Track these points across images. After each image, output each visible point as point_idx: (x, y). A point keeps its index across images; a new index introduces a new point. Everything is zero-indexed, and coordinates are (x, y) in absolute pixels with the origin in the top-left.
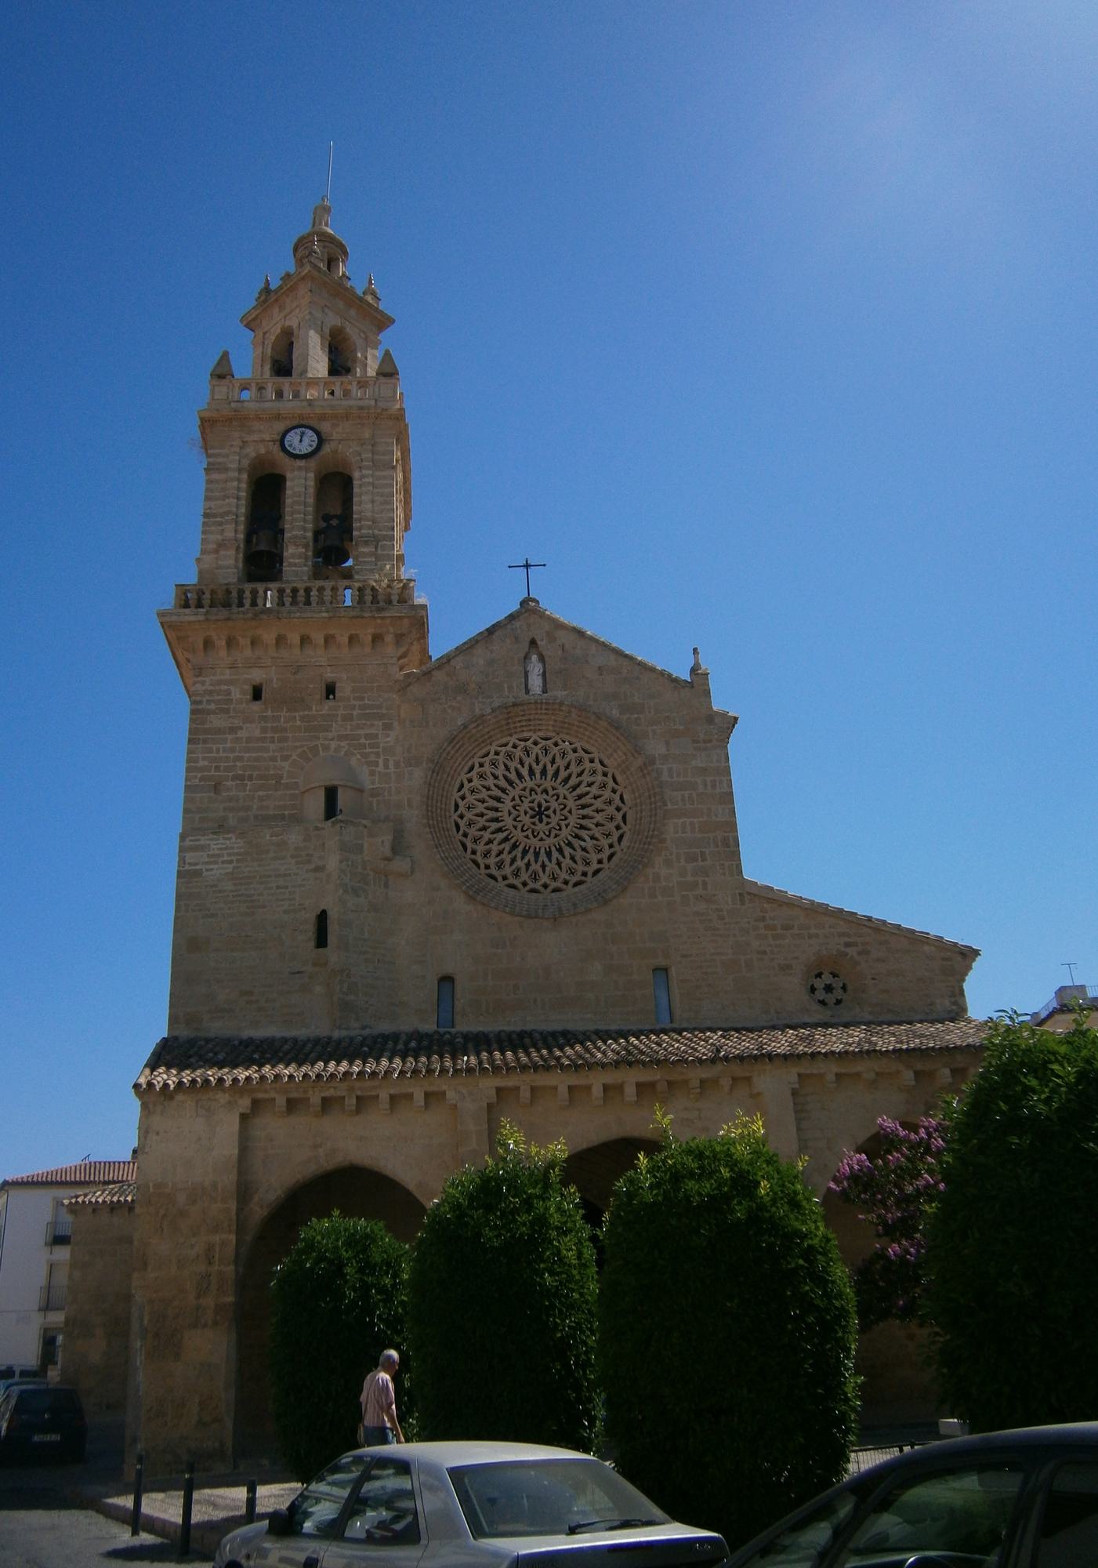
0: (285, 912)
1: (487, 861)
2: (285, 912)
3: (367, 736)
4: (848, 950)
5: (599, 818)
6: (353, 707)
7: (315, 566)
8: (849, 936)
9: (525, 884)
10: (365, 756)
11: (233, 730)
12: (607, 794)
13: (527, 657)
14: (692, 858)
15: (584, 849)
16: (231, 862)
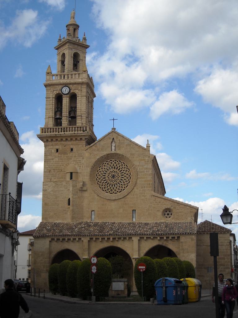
2: (62, 198)
3: (79, 161)
6: (76, 154)
7: (70, 121)
8: (172, 204)
9: (109, 192)
10: (78, 165)
11: (53, 159)
12: (127, 172)
13: (112, 142)
14: (142, 188)
15: (122, 185)
16: (52, 188)
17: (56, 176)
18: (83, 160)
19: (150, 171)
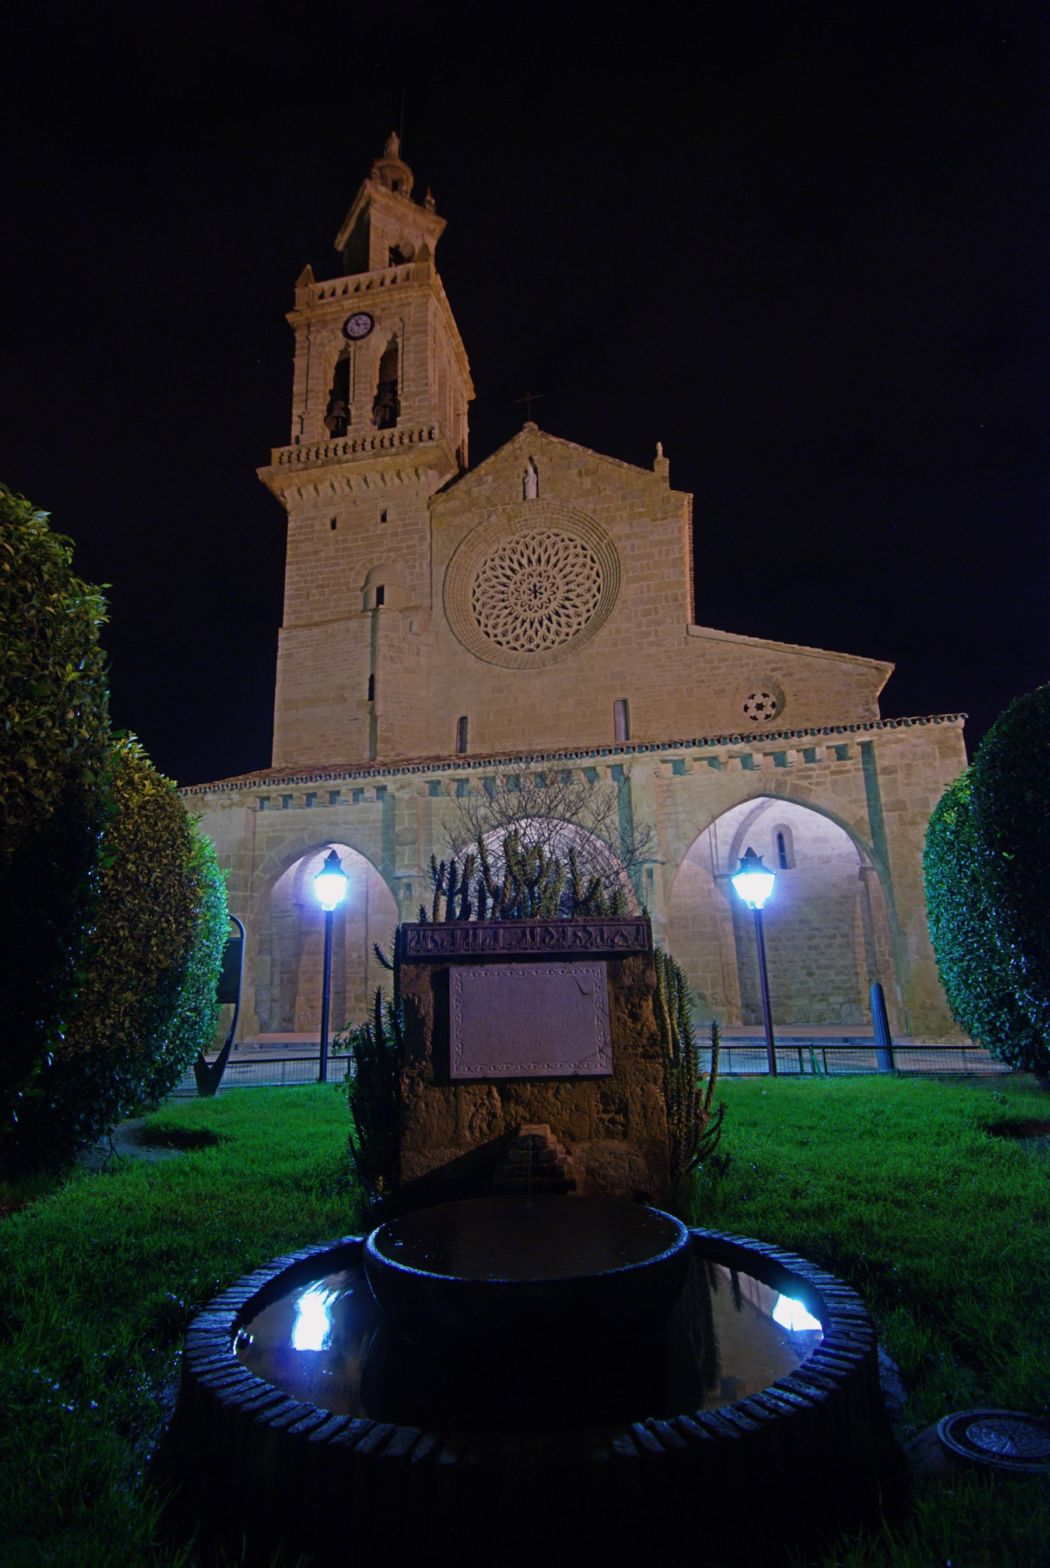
0: (348, 678)
1: (495, 632)
2: (348, 678)
3: (408, 547)
4: (773, 674)
5: (580, 590)
10: (407, 562)
11: (316, 553)
14: (647, 613)
15: (568, 616)
16: (311, 646)
17: (328, 608)
18: (423, 545)
19: (673, 550)
